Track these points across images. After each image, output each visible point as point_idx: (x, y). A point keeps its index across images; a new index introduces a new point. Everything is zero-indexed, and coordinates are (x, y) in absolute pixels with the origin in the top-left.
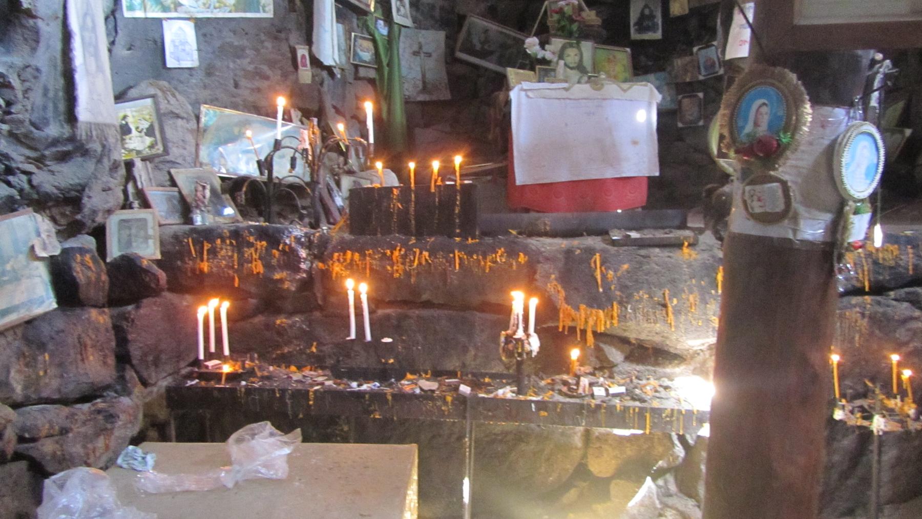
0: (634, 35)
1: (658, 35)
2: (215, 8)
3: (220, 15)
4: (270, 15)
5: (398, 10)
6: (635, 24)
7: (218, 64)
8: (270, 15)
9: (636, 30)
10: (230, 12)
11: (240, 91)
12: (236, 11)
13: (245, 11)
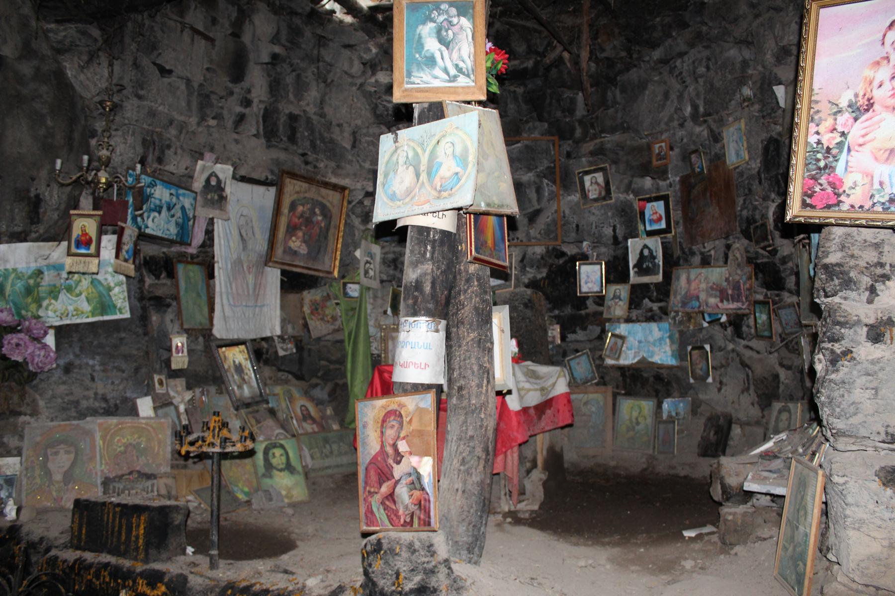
0: (634, 278)
1: (659, 278)
2: (73, 316)
3: (79, 321)
4: (127, 315)
5: (366, 272)
6: (634, 267)
7: (77, 362)
8: (127, 315)
9: (635, 272)
10: (88, 317)
11: (94, 386)
12: (93, 316)
13: (102, 315)
